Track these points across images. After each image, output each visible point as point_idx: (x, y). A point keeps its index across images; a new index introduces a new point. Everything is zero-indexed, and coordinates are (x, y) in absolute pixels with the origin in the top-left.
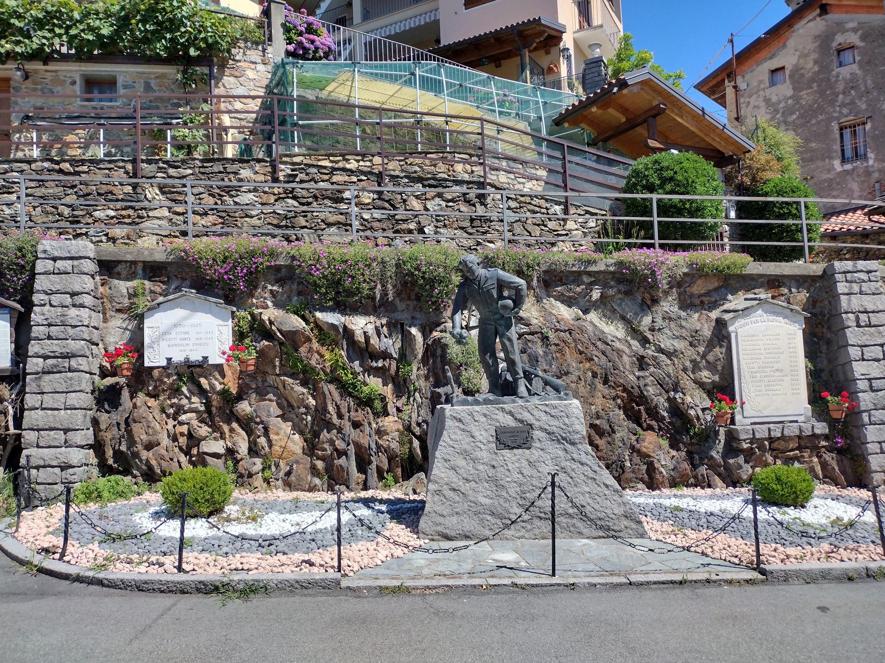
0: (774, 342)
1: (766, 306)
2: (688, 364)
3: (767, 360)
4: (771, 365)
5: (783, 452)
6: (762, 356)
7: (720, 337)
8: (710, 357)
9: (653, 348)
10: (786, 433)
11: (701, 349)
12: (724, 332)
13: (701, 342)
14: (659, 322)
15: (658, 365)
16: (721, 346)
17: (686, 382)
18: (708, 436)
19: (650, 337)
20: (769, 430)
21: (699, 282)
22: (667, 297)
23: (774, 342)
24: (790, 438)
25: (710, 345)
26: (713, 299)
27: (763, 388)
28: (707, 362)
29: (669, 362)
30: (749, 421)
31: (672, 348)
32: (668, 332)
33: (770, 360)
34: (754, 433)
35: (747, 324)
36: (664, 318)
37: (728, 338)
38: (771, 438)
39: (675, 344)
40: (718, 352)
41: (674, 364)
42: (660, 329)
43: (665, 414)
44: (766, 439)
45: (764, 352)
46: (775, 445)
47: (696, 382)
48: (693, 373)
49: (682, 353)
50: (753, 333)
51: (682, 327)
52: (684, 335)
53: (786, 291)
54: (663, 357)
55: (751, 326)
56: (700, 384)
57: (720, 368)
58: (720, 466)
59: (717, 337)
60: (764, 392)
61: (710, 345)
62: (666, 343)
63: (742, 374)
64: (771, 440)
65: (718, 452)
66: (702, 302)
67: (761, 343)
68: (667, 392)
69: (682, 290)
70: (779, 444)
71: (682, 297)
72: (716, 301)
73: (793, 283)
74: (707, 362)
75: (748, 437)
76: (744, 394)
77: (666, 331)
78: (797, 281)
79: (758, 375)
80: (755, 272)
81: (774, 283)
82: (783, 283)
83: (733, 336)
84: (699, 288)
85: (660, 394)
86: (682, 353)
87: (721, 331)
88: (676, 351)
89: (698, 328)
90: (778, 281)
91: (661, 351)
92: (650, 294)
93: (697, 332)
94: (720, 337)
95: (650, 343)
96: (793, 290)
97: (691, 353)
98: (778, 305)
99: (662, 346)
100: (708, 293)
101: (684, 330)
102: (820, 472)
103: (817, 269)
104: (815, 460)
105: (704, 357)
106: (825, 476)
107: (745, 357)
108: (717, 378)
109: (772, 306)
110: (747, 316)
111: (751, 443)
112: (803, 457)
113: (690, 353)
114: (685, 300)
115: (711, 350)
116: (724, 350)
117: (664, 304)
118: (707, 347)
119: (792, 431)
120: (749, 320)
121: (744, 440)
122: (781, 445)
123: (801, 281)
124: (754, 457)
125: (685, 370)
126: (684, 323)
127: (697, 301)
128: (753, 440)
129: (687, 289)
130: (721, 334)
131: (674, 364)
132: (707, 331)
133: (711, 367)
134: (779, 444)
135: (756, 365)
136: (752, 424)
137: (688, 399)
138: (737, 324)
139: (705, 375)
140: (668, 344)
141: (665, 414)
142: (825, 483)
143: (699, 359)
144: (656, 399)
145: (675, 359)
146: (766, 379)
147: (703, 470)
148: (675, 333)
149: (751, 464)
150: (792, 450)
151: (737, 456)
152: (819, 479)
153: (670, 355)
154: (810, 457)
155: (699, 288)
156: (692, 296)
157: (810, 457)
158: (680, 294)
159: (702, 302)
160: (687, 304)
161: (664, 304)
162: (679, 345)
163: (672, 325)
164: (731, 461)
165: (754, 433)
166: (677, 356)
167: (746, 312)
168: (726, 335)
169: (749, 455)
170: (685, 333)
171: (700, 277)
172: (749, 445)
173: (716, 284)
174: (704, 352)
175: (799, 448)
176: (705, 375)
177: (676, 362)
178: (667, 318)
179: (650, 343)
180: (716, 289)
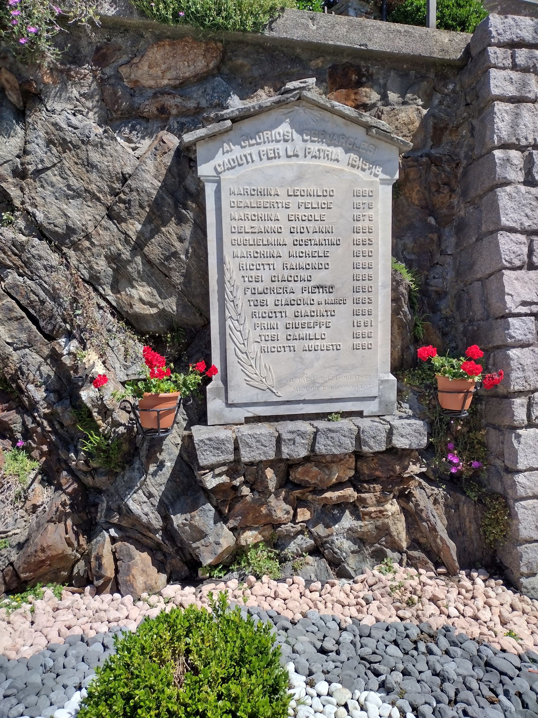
0: (317, 214)
1: (302, 113)
2: (101, 265)
3: (294, 262)
4: (304, 274)
5: (318, 491)
6: (283, 251)
7: (180, 194)
8: (154, 250)
9: (21, 223)
10: (321, 448)
11: (134, 227)
12: (189, 182)
13: (135, 209)
14: (39, 150)
15: (27, 268)
16: (181, 220)
17: (96, 314)
18: (135, 451)
19: (14, 192)
20: (279, 440)
21: (156, 54)
22: (65, 88)
23: (317, 214)
24: (336, 459)
25: (156, 218)
26: (191, 104)
27: (281, 333)
28: (147, 261)
29: (54, 259)
30: (241, 414)
31: (61, 221)
32: (56, 179)
33: (303, 261)
34: (237, 449)
35: (248, 160)
36: (49, 142)
37: (198, 196)
38: (281, 460)
39: (72, 212)
40: (174, 234)
41: (68, 266)
42: (38, 172)
43: (38, 394)
44: (271, 464)
45: (289, 239)
46: (297, 475)
47: (117, 312)
48: (116, 289)
49: (88, 237)
50: (261, 187)
51: (90, 166)
52: (93, 187)
53: (374, 97)
54: (40, 247)
55: (258, 165)
56: (132, 322)
57: (177, 278)
58: (156, 531)
59: (172, 194)
60: (283, 342)
61: (157, 215)
62: (50, 210)
63: (228, 296)
64: (286, 467)
65: (150, 496)
66: (163, 110)
67: (282, 214)
68: (50, 337)
69: (109, 71)
70: (306, 473)
71: (109, 90)
72: (199, 110)
73: (393, 79)
74: (147, 261)
75: (221, 458)
76: (230, 346)
77: (52, 176)
78: (404, 75)
79: (270, 299)
80: (297, 35)
81: (347, 71)
82: (370, 77)
83: (210, 190)
84: (155, 68)
85: (30, 344)
86: (88, 237)
87: (182, 177)
88: (71, 230)
89: (128, 170)
90: (358, 70)
91: (40, 232)
92: (19, 76)
93: (124, 179)
94: (180, 194)
95: (12, 209)
96: (393, 96)
97: (108, 235)
98: (332, 111)
99: (40, 216)
100: (181, 87)
101: (94, 176)
102: (403, 535)
103: (449, 44)
104: (392, 507)
105: (138, 247)
106: (415, 544)
107: (240, 250)
108: (171, 305)
109: (318, 113)
110: (249, 137)
111: (232, 473)
112: (362, 501)
113: (106, 237)
114: (116, 100)
115: (156, 231)
116: (187, 231)
117: (58, 107)
118: (149, 220)
119: (337, 439)
120: (254, 150)
121: (212, 468)
122: (312, 474)
123: (414, 73)
124: (239, 506)
125: (93, 282)
126: (95, 156)
127: (150, 107)
128: (234, 468)
129: (124, 71)
130: (182, 192)
131: (68, 266)
132: (150, 181)
133: (157, 274)
134: (306, 473)
135: (266, 274)
136: (248, 420)
137: (91, 357)
138: (220, 159)
139: (141, 296)
140: (54, 212)
141: (38, 394)
142: (412, 563)
143: (126, 254)
144: (15, 356)
145: (71, 253)
146: (290, 310)
147: (105, 545)
148: (73, 181)
149: (232, 523)
150: (339, 485)
151: (194, 507)
152: (401, 552)
153: (61, 239)
154: (379, 502)
155: (155, 68)
156: (136, 90)
157: (379, 502)
158: (102, 82)
159: (163, 110)
160: (122, 112)
161: (58, 107)
162: (81, 214)
163: (69, 160)
164: (178, 520)
165: (237, 449)
166: (75, 246)
167: (246, 126)
168: (193, 188)
169: (225, 503)
170: (96, 183)
171: (159, 38)
172: (225, 479)
173: (201, 65)
174: (140, 234)
175: (355, 482)
176: (141, 296)
177: (73, 261)
178: (58, 142)
179: (12, 209)
180: (202, 79)
